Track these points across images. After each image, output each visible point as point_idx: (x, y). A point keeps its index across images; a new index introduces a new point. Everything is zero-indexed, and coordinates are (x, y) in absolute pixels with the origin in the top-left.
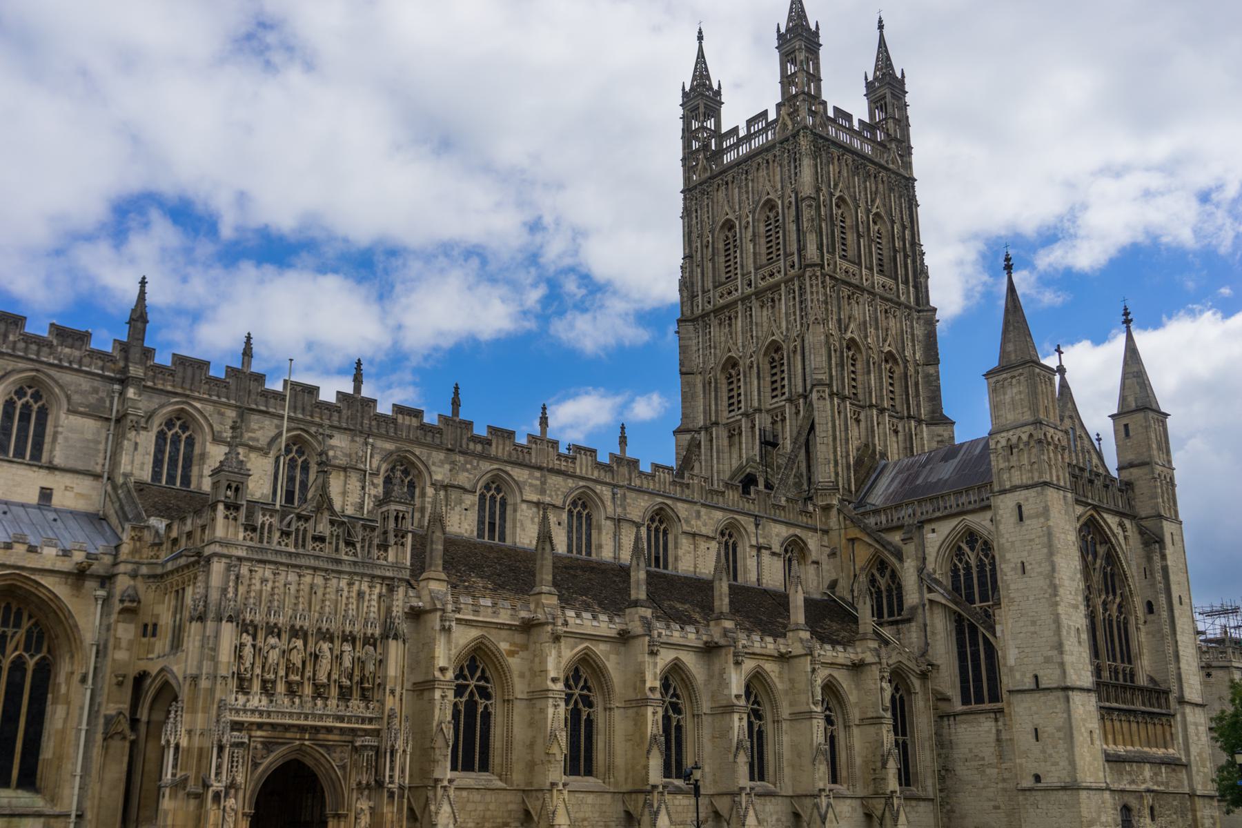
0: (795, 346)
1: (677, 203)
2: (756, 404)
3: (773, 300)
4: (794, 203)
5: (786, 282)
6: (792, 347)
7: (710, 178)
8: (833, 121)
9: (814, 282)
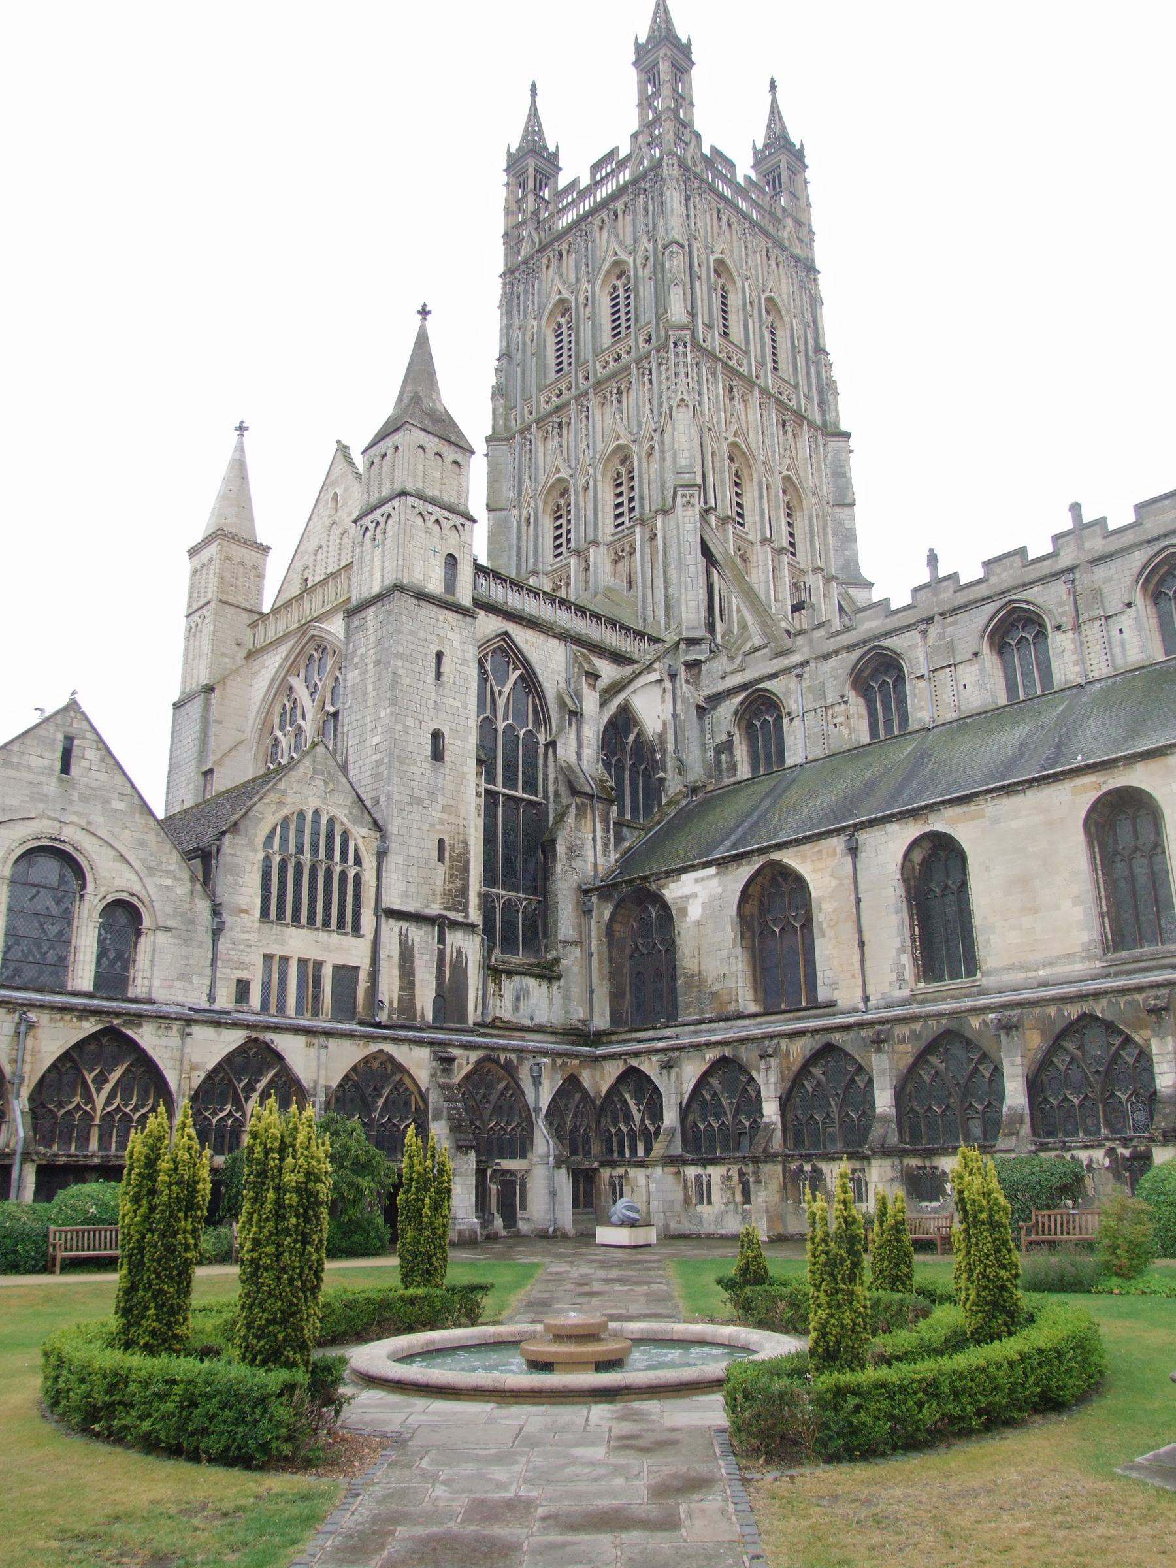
0: (652, 448)
1: (494, 289)
2: (591, 537)
3: (619, 389)
4: (651, 259)
5: (638, 362)
6: (646, 447)
7: (538, 251)
8: (709, 162)
9: (681, 349)
